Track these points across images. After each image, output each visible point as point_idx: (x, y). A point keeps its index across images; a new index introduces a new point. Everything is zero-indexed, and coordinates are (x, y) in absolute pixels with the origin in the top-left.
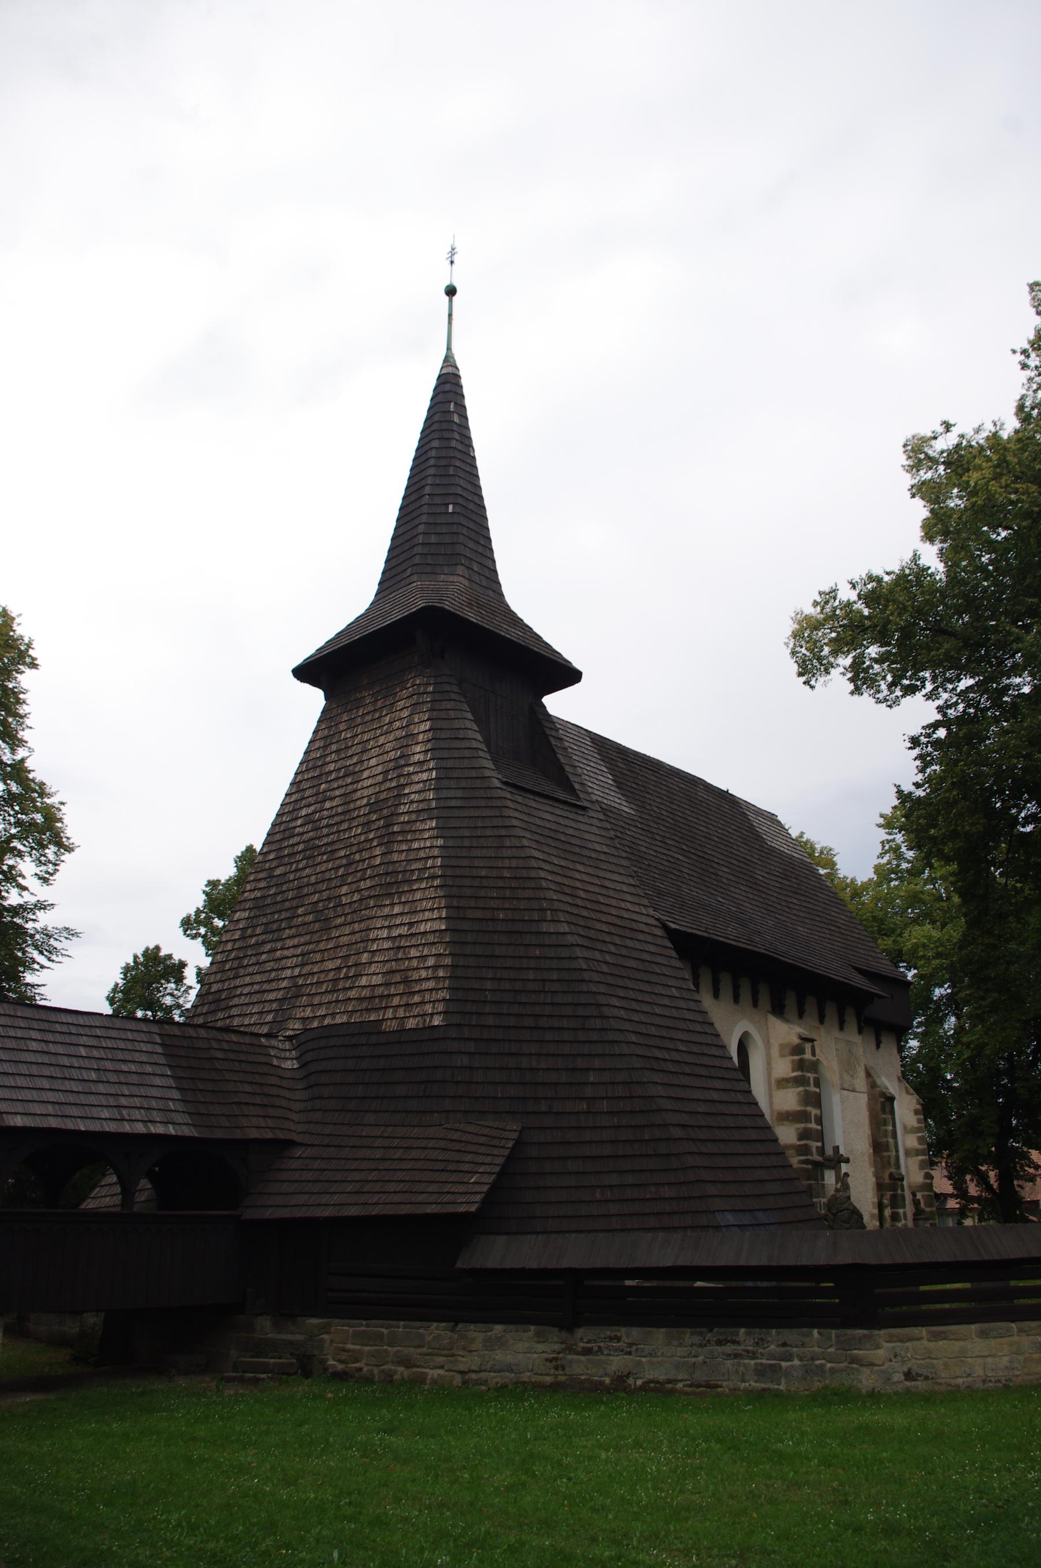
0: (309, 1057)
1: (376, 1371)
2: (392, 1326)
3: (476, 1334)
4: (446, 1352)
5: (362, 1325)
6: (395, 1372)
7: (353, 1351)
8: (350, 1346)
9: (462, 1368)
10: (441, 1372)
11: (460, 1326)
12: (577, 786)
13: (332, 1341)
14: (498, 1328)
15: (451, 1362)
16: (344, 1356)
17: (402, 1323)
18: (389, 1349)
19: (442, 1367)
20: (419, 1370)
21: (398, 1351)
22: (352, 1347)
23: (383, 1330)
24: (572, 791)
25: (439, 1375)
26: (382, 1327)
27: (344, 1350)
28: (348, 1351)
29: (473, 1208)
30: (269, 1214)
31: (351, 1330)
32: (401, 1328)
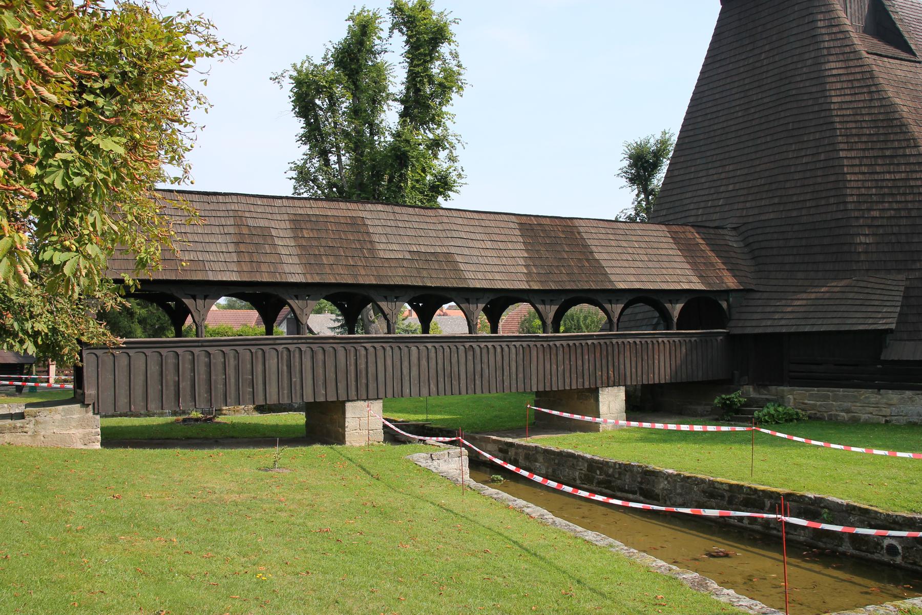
0: (751, 240)
1: (825, 415)
2: (835, 391)
3: (893, 396)
4: (873, 405)
5: (814, 390)
6: (838, 415)
7: (809, 404)
8: (806, 401)
9: (884, 413)
10: (870, 415)
11: (882, 391)
12: (913, 47)
13: (795, 399)
14: (908, 393)
15: (877, 410)
16: (803, 406)
17: (841, 389)
18: (834, 403)
19: (871, 413)
20: (855, 414)
21: (841, 404)
22: (809, 402)
23: (829, 393)
24: (909, 50)
25: (869, 417)
26: (829, 391)
27: (804, 403)
28: (806, 404)
29: (893, 326)
30: (748, 331)
31: (808, 393)
32: (841, 391)
